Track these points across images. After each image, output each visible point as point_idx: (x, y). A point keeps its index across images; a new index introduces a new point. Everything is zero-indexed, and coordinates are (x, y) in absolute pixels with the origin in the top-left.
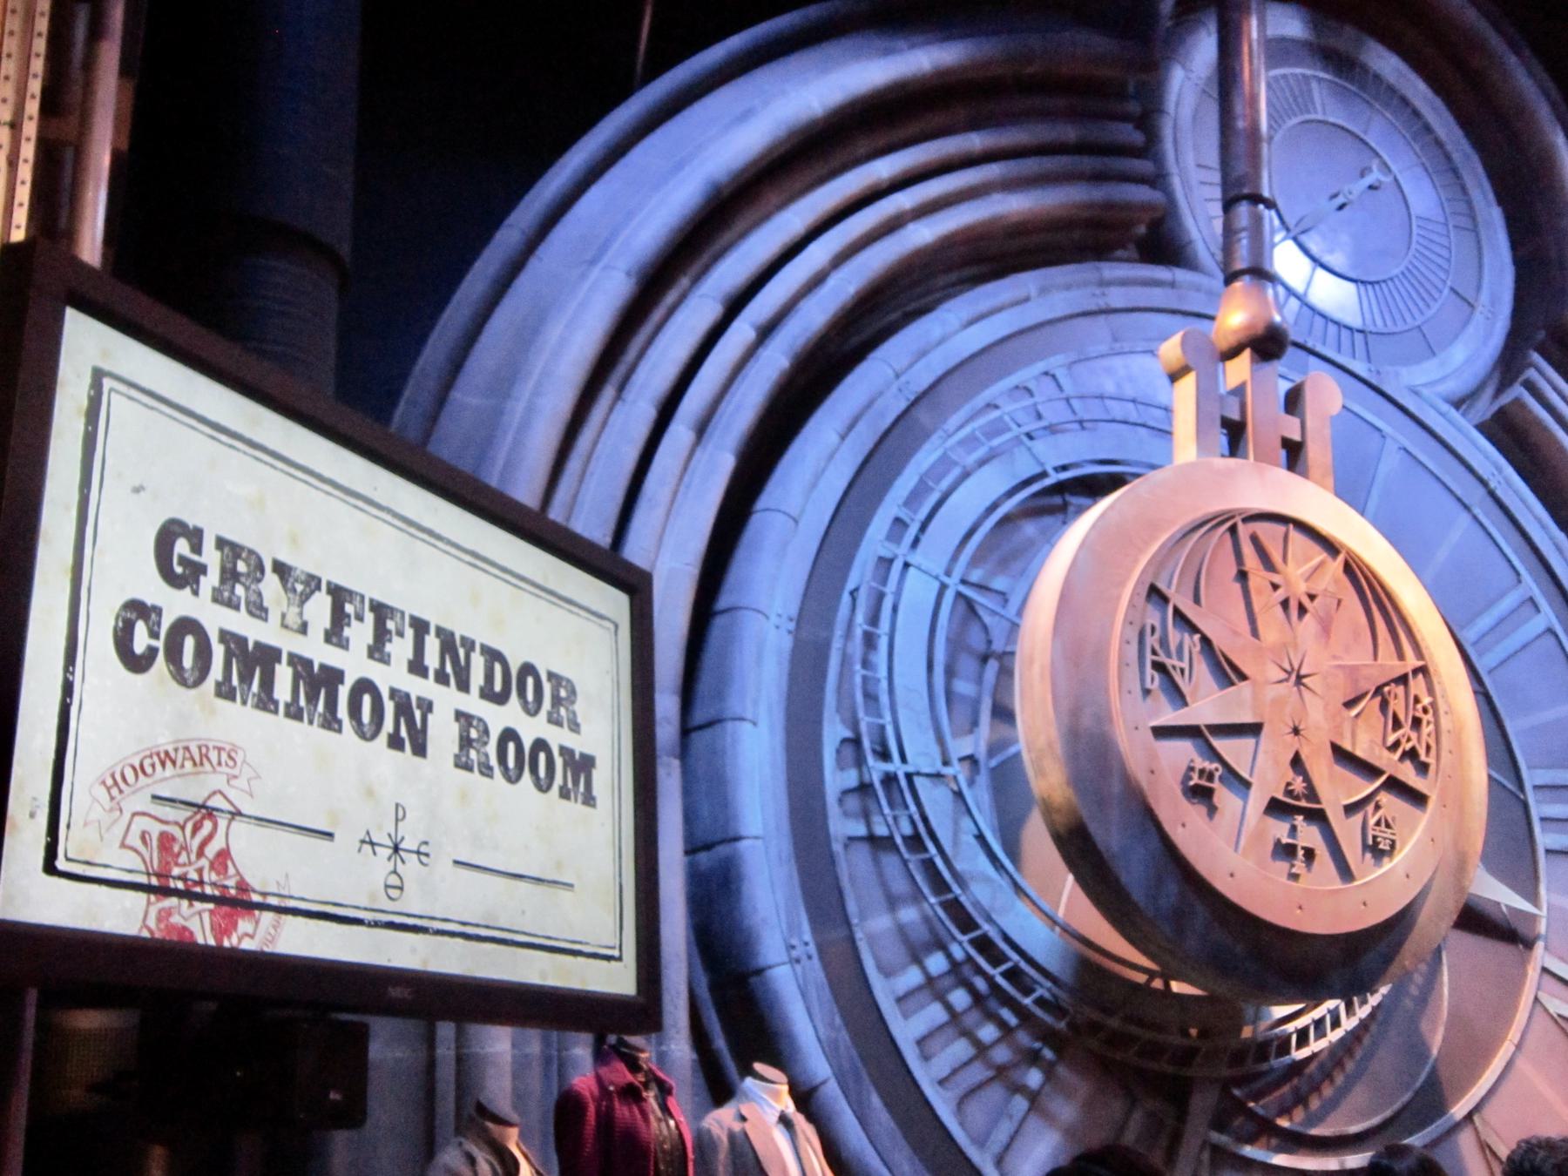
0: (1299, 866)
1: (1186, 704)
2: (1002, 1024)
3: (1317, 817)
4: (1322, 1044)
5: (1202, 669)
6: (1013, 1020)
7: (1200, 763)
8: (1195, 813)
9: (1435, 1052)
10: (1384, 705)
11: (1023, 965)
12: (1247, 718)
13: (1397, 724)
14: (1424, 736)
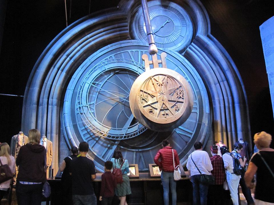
1: (147, 102)
3: (168, 109)
8: (151, 114)
12: (156, 101)
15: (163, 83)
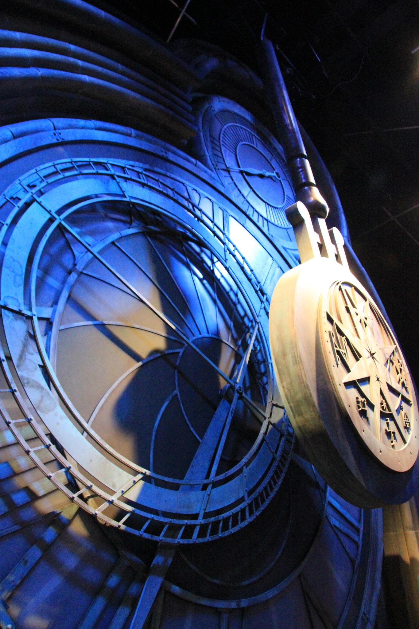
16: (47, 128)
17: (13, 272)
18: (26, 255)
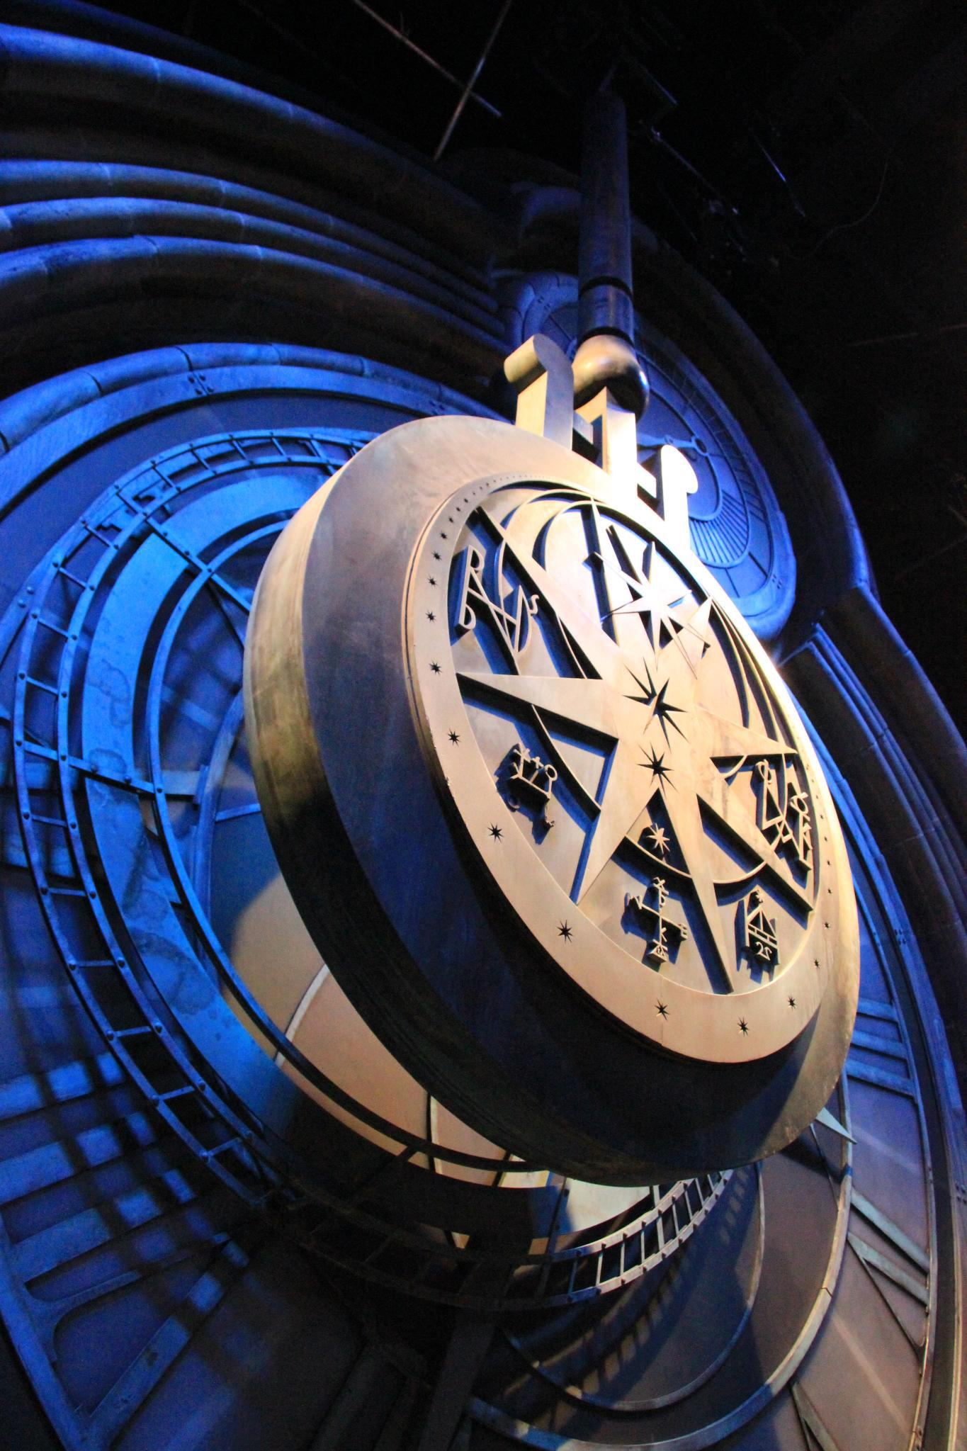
0: (660, 951)
2: (164, 1195)
3: (684, 889)
4: (629, 1275)
5: (535, 631)
6: (185, 1193)
7: (525, 755)
9: (750, 1303)
10: (757, 783)
11: (209, 1093)
13: (773, 812)
14: (801, 836)
15: (678, 628)
16: (176, 367)
17: (108, 693)
18: (136, 654)
